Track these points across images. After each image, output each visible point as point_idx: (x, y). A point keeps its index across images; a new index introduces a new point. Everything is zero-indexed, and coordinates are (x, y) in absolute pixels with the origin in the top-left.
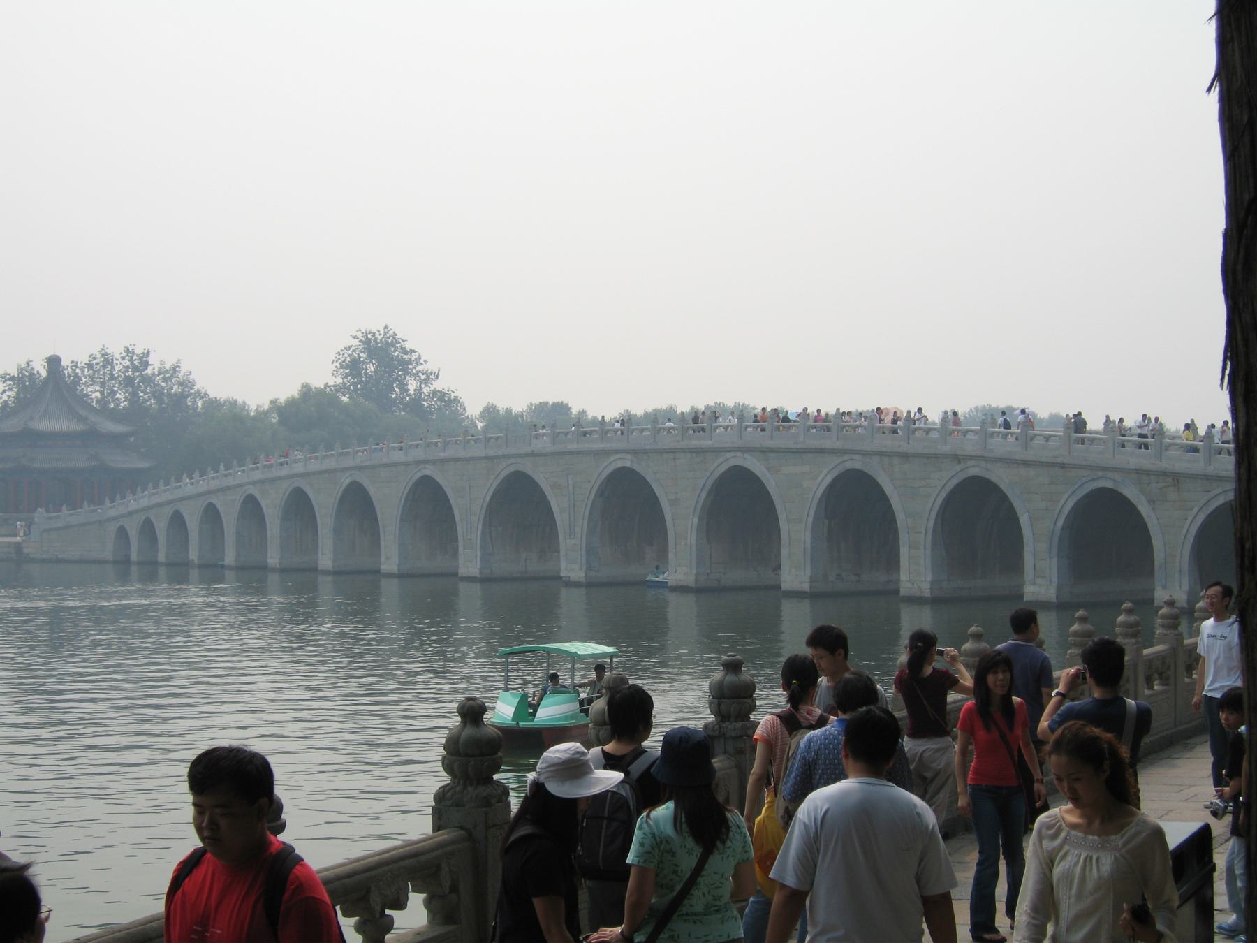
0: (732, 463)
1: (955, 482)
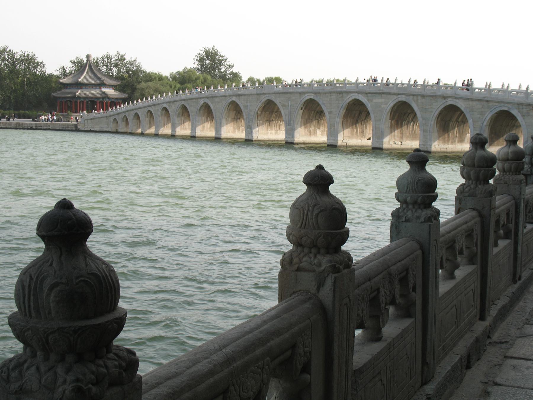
0: (354, 98)
1: (443, 106)
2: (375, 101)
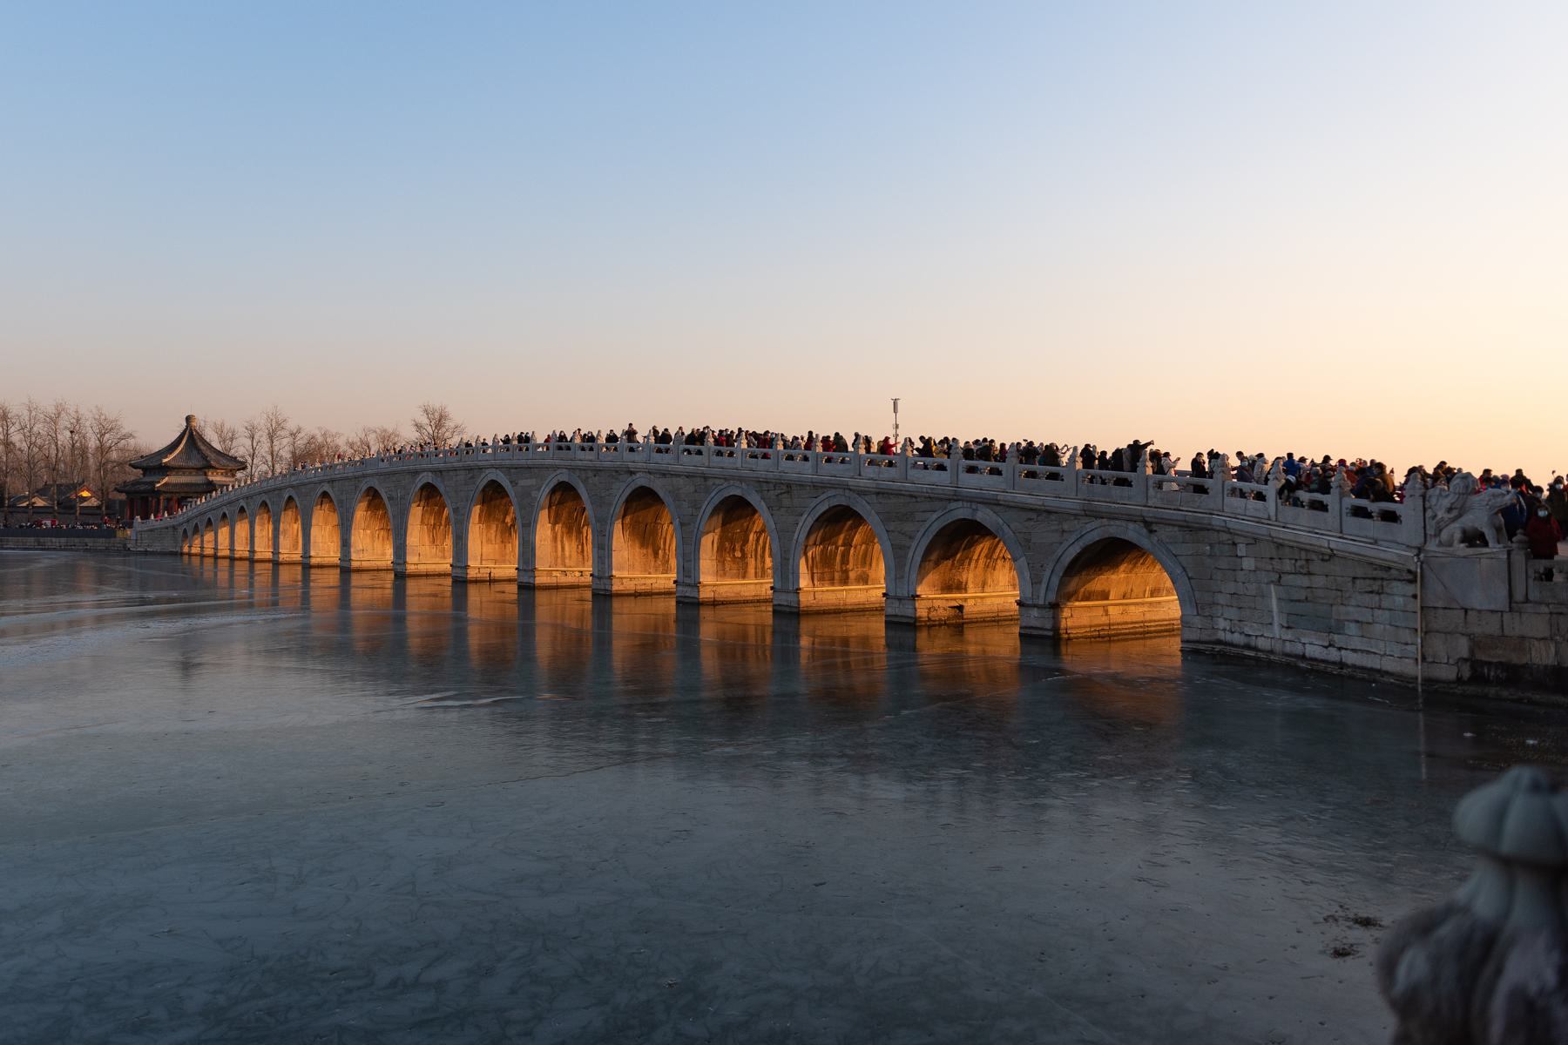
2: (522, 483)
